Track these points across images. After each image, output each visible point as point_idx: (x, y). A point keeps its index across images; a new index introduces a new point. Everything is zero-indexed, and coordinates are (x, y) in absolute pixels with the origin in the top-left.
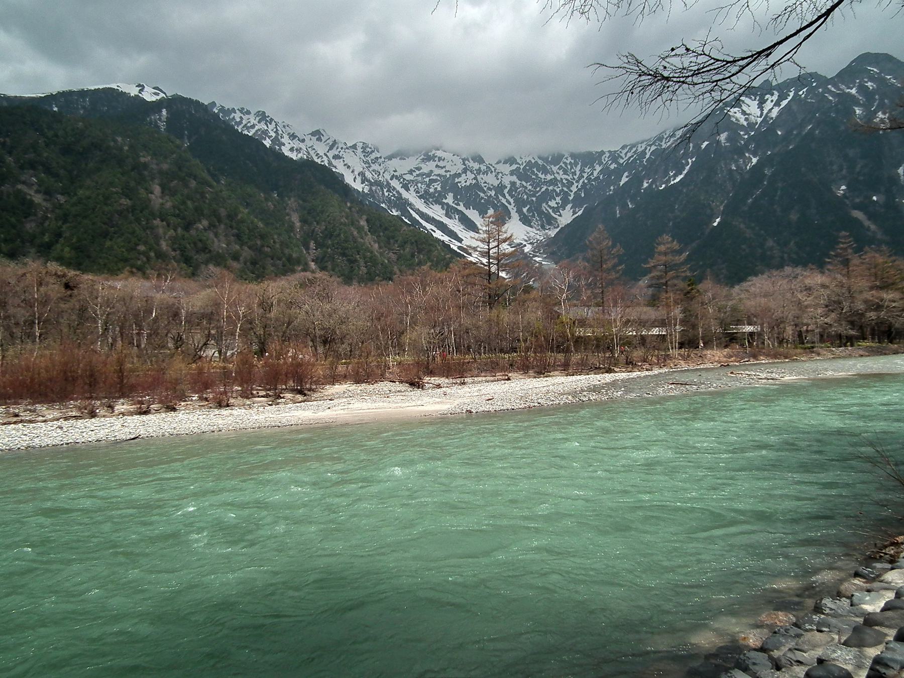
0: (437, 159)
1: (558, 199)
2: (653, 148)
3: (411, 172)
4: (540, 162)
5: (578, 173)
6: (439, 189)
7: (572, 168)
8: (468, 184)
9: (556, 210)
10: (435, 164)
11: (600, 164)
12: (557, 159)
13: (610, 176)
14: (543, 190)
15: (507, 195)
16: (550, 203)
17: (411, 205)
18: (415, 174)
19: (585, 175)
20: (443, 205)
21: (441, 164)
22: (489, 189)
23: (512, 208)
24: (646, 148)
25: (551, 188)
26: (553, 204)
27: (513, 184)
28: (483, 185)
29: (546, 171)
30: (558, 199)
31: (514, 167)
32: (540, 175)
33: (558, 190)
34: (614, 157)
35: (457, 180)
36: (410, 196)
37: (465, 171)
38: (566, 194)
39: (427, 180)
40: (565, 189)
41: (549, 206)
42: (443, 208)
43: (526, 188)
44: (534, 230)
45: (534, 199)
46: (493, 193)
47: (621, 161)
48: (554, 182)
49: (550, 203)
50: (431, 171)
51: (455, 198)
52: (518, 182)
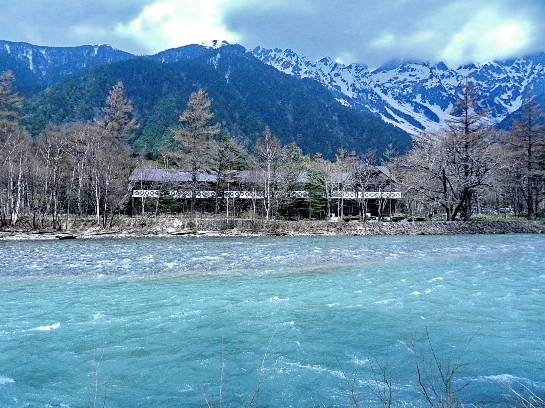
0: (410, 70)
1: (510, 93)
3: (390, 81)
4: (495, 65)
5: (529, 71)
6: (411, 92)
8: (433, 86)
10: (409, 73)
12: (509, 62)
14: (497, 86)
16: (502, 96)
17: (387, 105)
18: (393, 82)
19: (536, 72)
20: (411, 102)
21: (413, 73)
22: (451, 89)
25: (503, 84)
26: (505, 96)
28: (445, 86)
29: (499, 71)
30: (510, 93)
31: (473, 70)
33: (510, 86)
36: (389, 99)
37: (431, 77)
38: (517, 88)
39: (402, 86)
40: (516, 84)
42: (412, 105)
43: (482, 86)
45: (488, 94)
46: (453, 92)
48: (506, 80)
49: (502, 96)
50: (406, 79)
51: (423, 97)
52: (475, 82)
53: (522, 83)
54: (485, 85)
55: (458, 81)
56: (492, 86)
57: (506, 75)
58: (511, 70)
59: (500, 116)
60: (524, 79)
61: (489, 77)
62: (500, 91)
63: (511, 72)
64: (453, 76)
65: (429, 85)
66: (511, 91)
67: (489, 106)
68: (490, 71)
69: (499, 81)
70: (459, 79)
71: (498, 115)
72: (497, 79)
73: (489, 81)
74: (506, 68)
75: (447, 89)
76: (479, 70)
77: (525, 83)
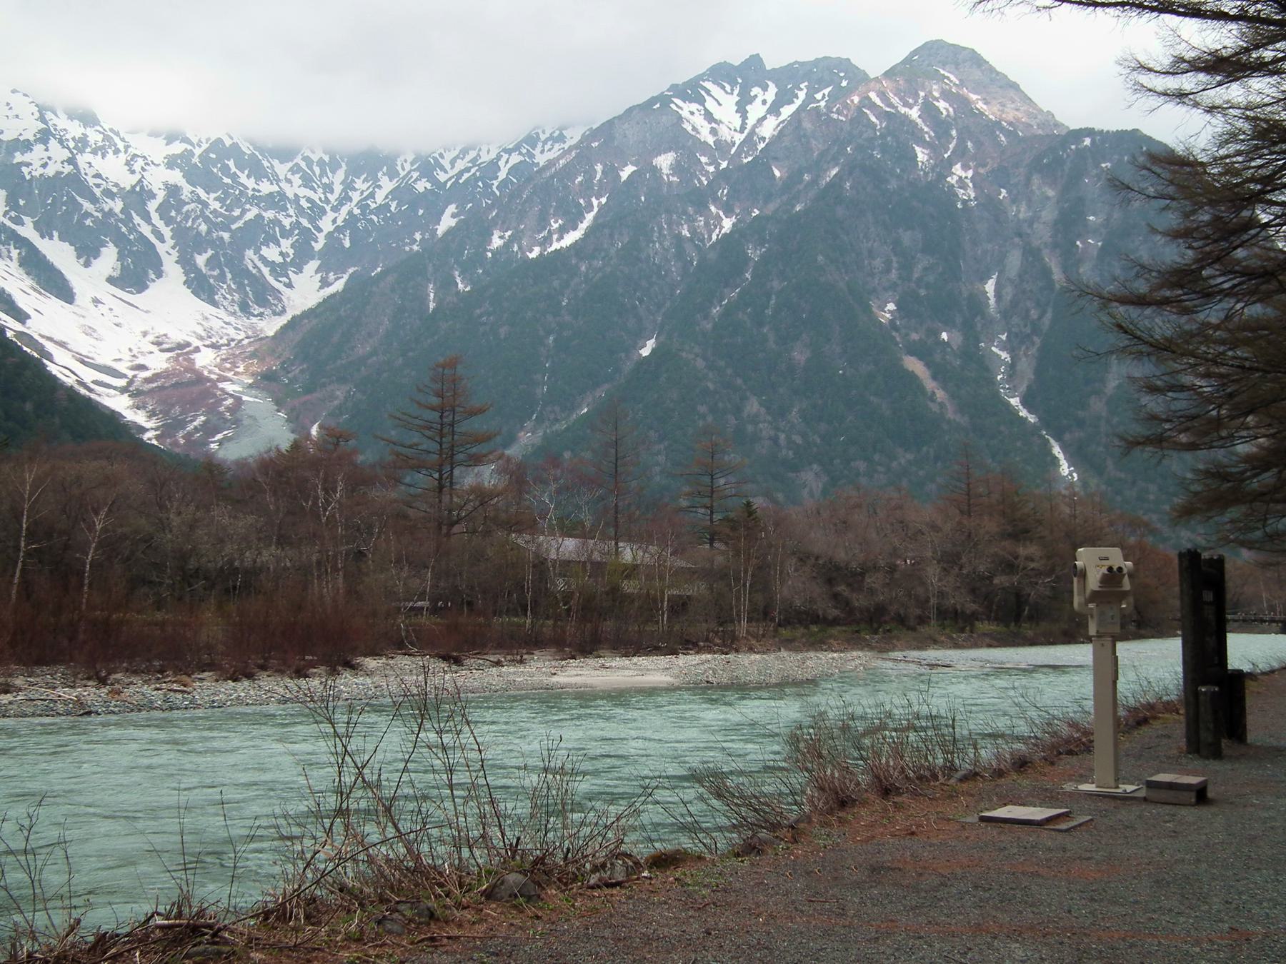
1: (286, 244)
2: (515, 158)
5: (338, 188)
7: (323, 173)
8: (50, 171)
9: (279, 270)
11: (392, 174)
13: (413, 206)
14: (250, 216)
15: (155, 218)
16: (265, 251)
19: (356, 197)
23: (167, 251)
24: (499, 157)
25: (269, 215)
26: (271, 253)
27: (173, 190)
28: (91, 181)
29: (258, 172)
30: (286, 244)
31: (178, 148)
32: (243, 178)
33: (287, 223)
34: (427, 167)
35: (18, 158)
37: (44, 136)
38: (305, 239)
40: (305, 222)
41: (263, 259)
43: (205, 204)
44: (221, 313)
45: (226, 236)
46: (117, 205)
47: (442, 177)
49: (265, 251)
53: (321, 224)
54: (216, 205)
55: (133, 172)
56: (237, 213)
57: (275, 188)
58: (289, 176)
59: (261, 315)
60: (324, 212)
61: (226, 180)
62: (259, 233)
63: (289, 181)
64: (117, 152)
65: (37, 164)
66: (290, 241)
67: (229, 276)
68: (231, 163)
69: (256, 199)
70: (138, 165)
71: (257, 310)
72: (250, 193)
73: (226, 194)
74: (276, 163)
75: (97, 192)
76: (198, 151)
77: (326, 225)
